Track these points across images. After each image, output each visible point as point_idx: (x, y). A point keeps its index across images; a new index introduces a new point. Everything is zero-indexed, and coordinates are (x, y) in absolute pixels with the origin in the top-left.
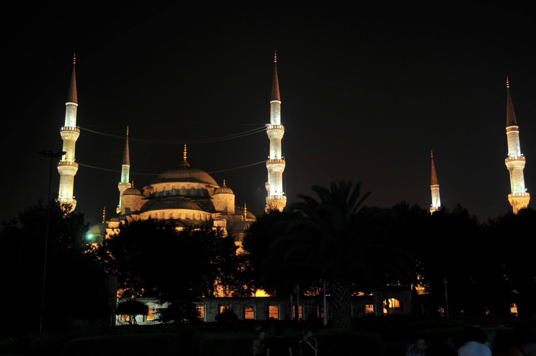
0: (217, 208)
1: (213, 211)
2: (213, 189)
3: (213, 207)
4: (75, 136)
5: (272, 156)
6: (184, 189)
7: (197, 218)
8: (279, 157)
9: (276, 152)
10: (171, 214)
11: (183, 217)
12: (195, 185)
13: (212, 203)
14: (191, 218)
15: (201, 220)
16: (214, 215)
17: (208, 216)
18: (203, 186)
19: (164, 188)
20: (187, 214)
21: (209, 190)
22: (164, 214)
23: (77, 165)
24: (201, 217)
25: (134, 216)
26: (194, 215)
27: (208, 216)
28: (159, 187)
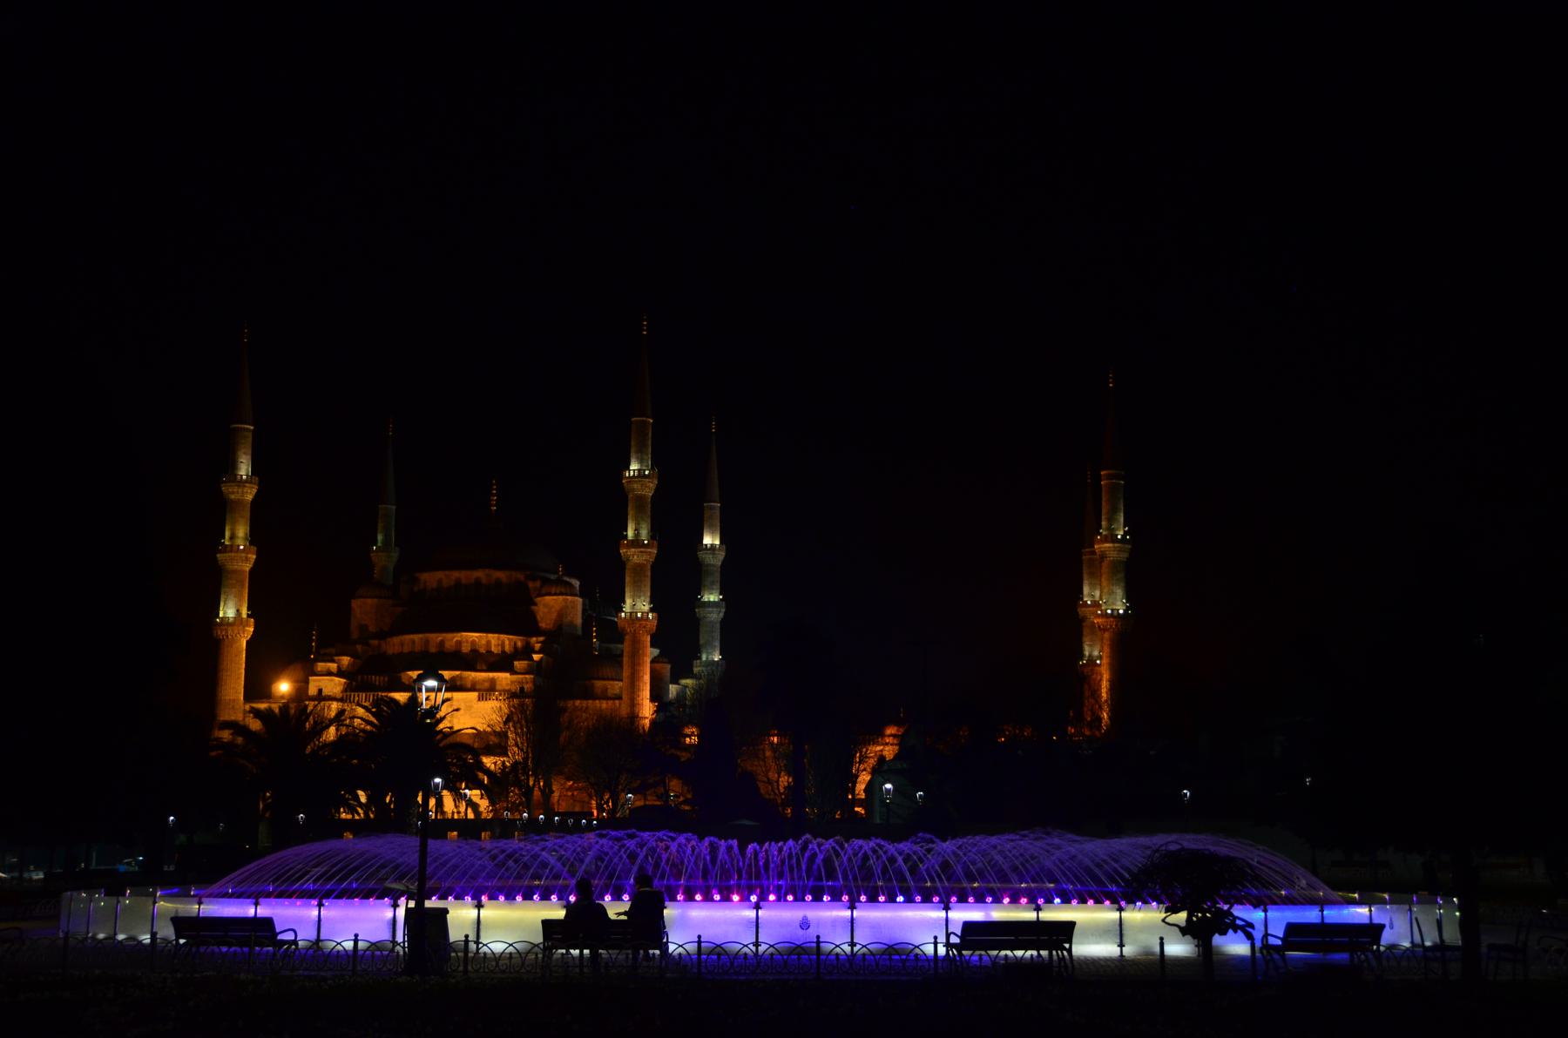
0: (543, 625)
1: (537, 632)
2: (538, 584)
3: (536, 622)
4: (249, 494)
5: (630, 533)
6: (478, 582)
7: (493, 649)
8: (644, 534)
9: (638, 524)
10: (442, 642)
11: (466, 649)
12: (502, 575)
13: (533, 616)
14: (482, 650)
15: (503, 651)
16: (534, 639)
17: (519, 644)
18: (520, 576)
19: (440, 581)
20: (473, 642)
21: (531, 585)
22: (427, 642)
23: (254, 548)
24: (503, 645)
25: (375, 642)
26: (489, 643)
27: (519, 644)
28: (431, 579)
